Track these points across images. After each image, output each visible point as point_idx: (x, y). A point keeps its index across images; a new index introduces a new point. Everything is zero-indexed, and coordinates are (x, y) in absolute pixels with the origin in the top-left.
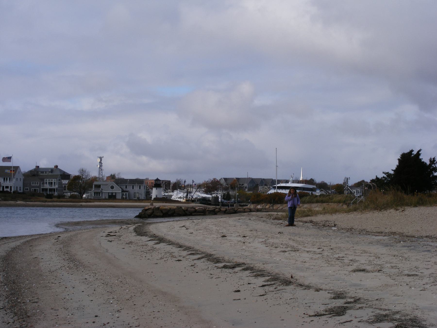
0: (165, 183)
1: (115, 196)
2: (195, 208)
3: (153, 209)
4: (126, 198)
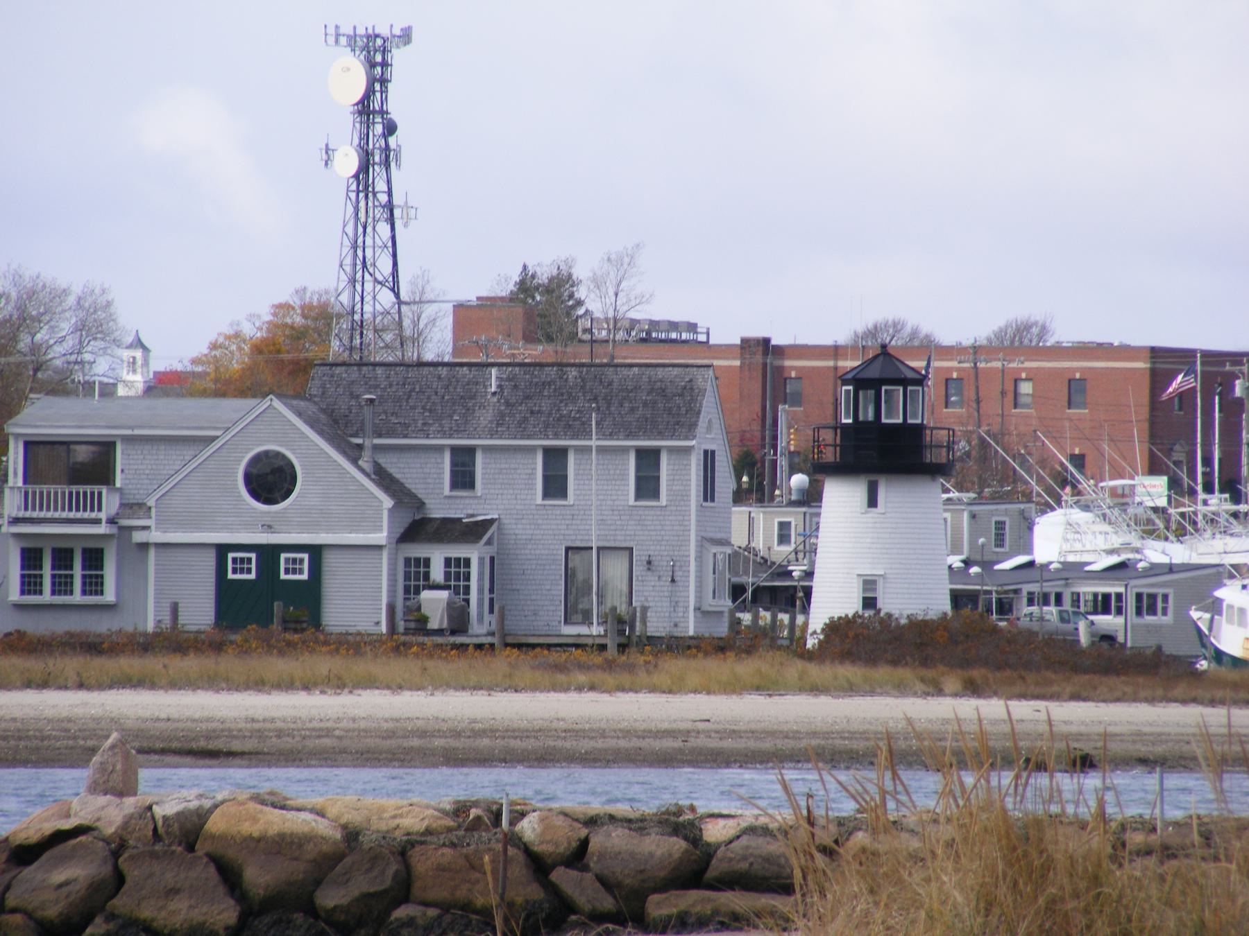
1: (309, 596)
3: (118, 847)
4: (459, 621)
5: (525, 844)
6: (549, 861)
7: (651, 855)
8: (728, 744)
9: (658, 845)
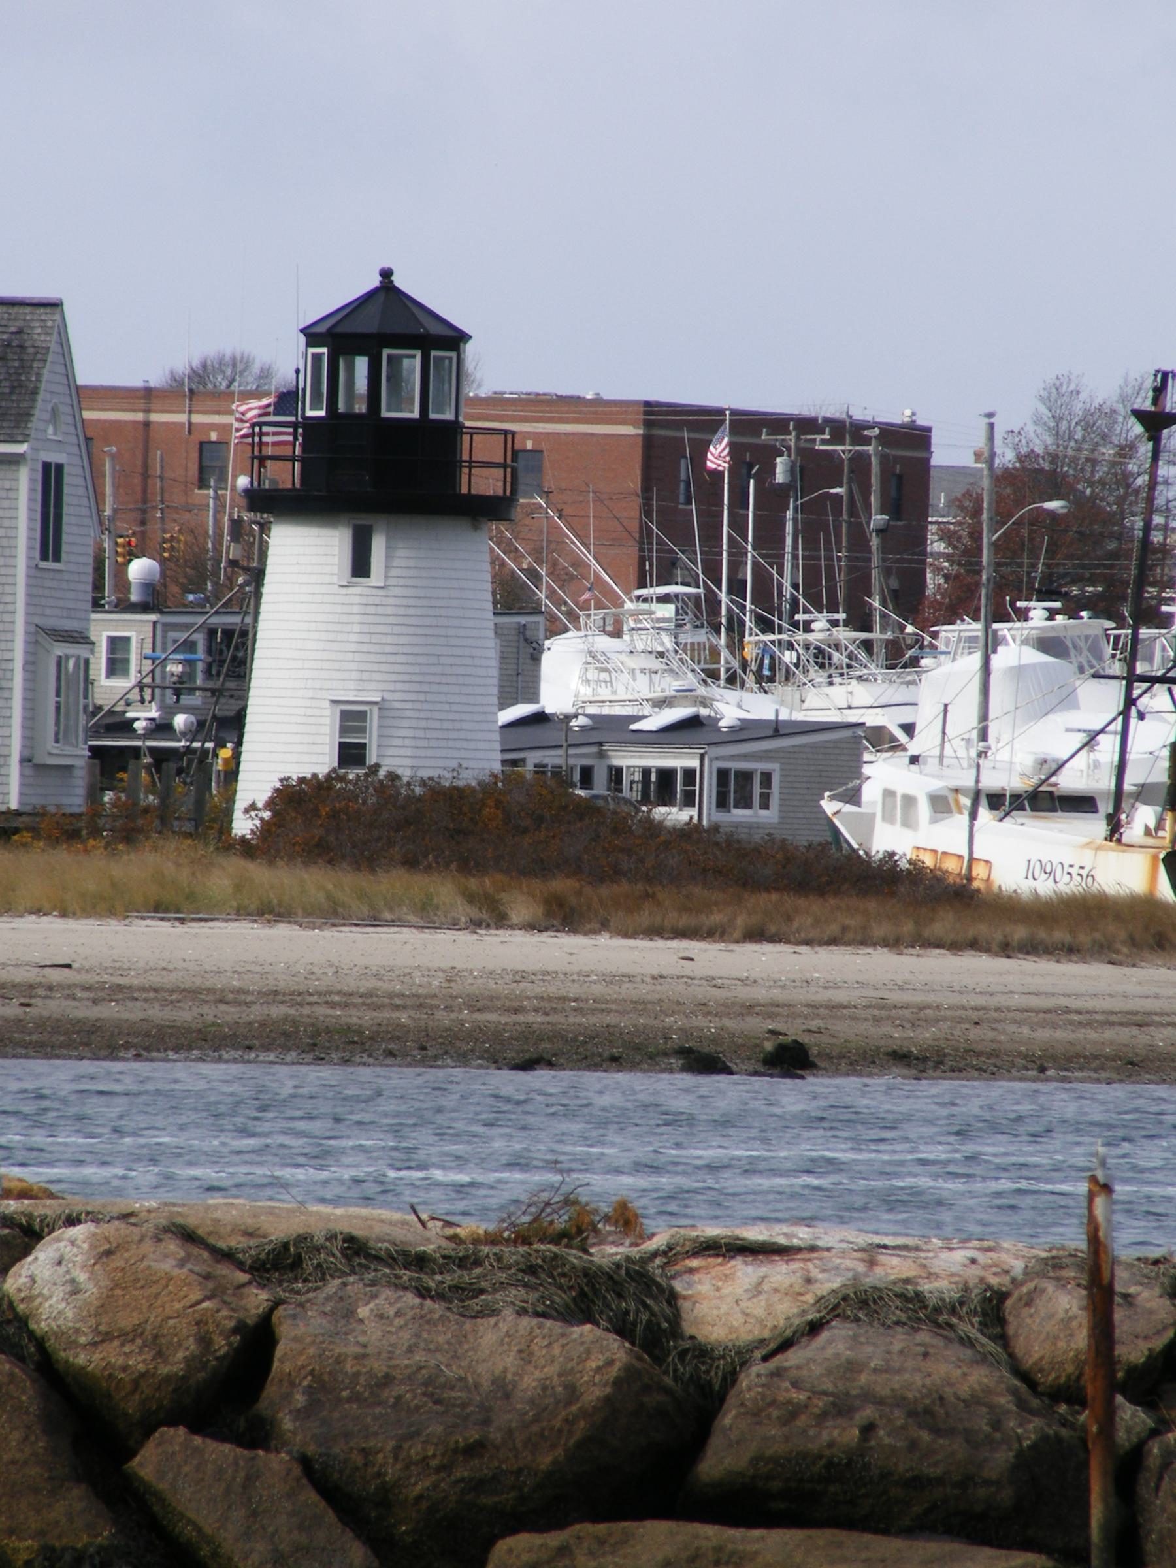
0: (815, 470)
2: (635, 1303)
5: (40, 1342)
6: (132, 1407)
7: (503, 1388)
8: (110, 1011)
9: (526, 1355)
